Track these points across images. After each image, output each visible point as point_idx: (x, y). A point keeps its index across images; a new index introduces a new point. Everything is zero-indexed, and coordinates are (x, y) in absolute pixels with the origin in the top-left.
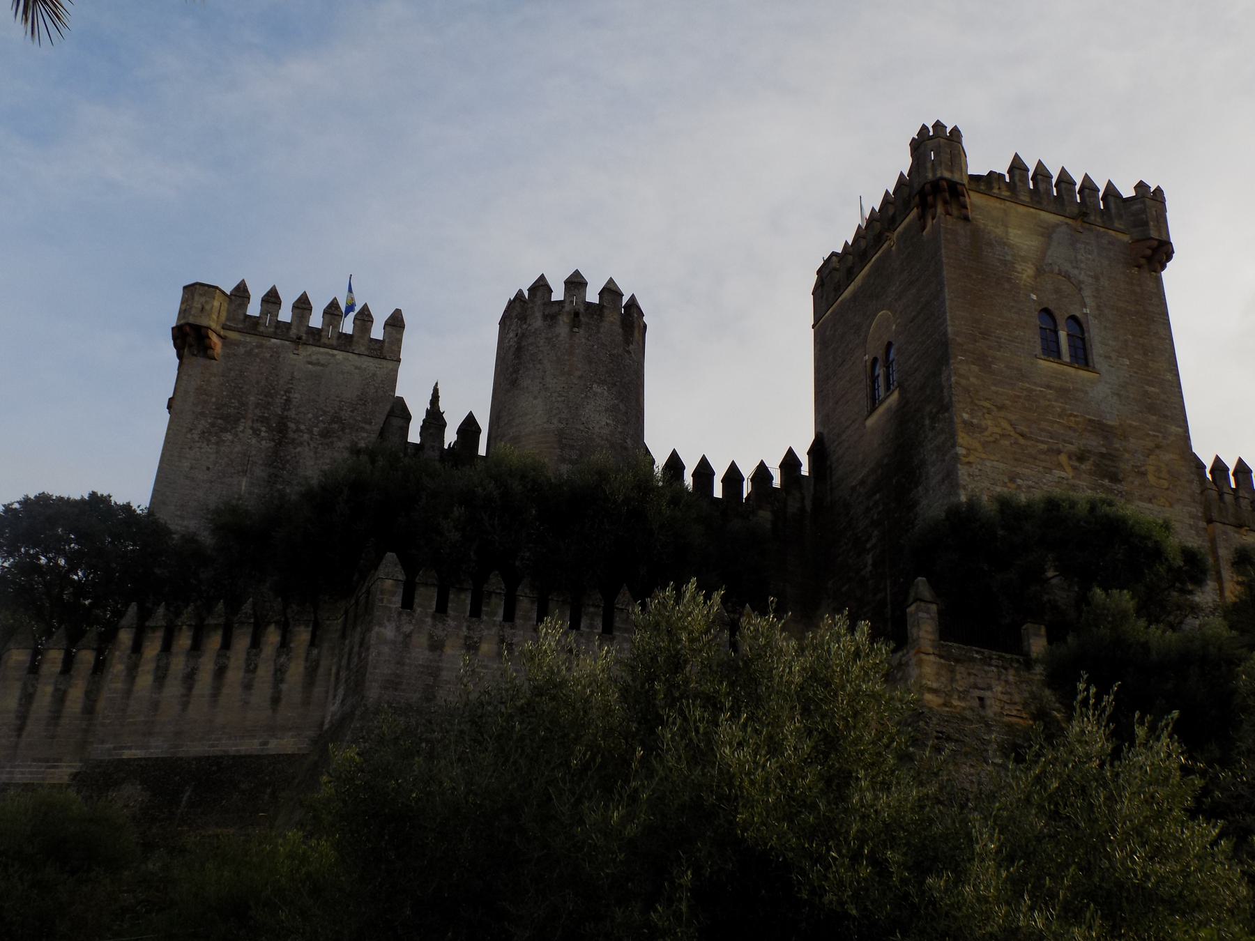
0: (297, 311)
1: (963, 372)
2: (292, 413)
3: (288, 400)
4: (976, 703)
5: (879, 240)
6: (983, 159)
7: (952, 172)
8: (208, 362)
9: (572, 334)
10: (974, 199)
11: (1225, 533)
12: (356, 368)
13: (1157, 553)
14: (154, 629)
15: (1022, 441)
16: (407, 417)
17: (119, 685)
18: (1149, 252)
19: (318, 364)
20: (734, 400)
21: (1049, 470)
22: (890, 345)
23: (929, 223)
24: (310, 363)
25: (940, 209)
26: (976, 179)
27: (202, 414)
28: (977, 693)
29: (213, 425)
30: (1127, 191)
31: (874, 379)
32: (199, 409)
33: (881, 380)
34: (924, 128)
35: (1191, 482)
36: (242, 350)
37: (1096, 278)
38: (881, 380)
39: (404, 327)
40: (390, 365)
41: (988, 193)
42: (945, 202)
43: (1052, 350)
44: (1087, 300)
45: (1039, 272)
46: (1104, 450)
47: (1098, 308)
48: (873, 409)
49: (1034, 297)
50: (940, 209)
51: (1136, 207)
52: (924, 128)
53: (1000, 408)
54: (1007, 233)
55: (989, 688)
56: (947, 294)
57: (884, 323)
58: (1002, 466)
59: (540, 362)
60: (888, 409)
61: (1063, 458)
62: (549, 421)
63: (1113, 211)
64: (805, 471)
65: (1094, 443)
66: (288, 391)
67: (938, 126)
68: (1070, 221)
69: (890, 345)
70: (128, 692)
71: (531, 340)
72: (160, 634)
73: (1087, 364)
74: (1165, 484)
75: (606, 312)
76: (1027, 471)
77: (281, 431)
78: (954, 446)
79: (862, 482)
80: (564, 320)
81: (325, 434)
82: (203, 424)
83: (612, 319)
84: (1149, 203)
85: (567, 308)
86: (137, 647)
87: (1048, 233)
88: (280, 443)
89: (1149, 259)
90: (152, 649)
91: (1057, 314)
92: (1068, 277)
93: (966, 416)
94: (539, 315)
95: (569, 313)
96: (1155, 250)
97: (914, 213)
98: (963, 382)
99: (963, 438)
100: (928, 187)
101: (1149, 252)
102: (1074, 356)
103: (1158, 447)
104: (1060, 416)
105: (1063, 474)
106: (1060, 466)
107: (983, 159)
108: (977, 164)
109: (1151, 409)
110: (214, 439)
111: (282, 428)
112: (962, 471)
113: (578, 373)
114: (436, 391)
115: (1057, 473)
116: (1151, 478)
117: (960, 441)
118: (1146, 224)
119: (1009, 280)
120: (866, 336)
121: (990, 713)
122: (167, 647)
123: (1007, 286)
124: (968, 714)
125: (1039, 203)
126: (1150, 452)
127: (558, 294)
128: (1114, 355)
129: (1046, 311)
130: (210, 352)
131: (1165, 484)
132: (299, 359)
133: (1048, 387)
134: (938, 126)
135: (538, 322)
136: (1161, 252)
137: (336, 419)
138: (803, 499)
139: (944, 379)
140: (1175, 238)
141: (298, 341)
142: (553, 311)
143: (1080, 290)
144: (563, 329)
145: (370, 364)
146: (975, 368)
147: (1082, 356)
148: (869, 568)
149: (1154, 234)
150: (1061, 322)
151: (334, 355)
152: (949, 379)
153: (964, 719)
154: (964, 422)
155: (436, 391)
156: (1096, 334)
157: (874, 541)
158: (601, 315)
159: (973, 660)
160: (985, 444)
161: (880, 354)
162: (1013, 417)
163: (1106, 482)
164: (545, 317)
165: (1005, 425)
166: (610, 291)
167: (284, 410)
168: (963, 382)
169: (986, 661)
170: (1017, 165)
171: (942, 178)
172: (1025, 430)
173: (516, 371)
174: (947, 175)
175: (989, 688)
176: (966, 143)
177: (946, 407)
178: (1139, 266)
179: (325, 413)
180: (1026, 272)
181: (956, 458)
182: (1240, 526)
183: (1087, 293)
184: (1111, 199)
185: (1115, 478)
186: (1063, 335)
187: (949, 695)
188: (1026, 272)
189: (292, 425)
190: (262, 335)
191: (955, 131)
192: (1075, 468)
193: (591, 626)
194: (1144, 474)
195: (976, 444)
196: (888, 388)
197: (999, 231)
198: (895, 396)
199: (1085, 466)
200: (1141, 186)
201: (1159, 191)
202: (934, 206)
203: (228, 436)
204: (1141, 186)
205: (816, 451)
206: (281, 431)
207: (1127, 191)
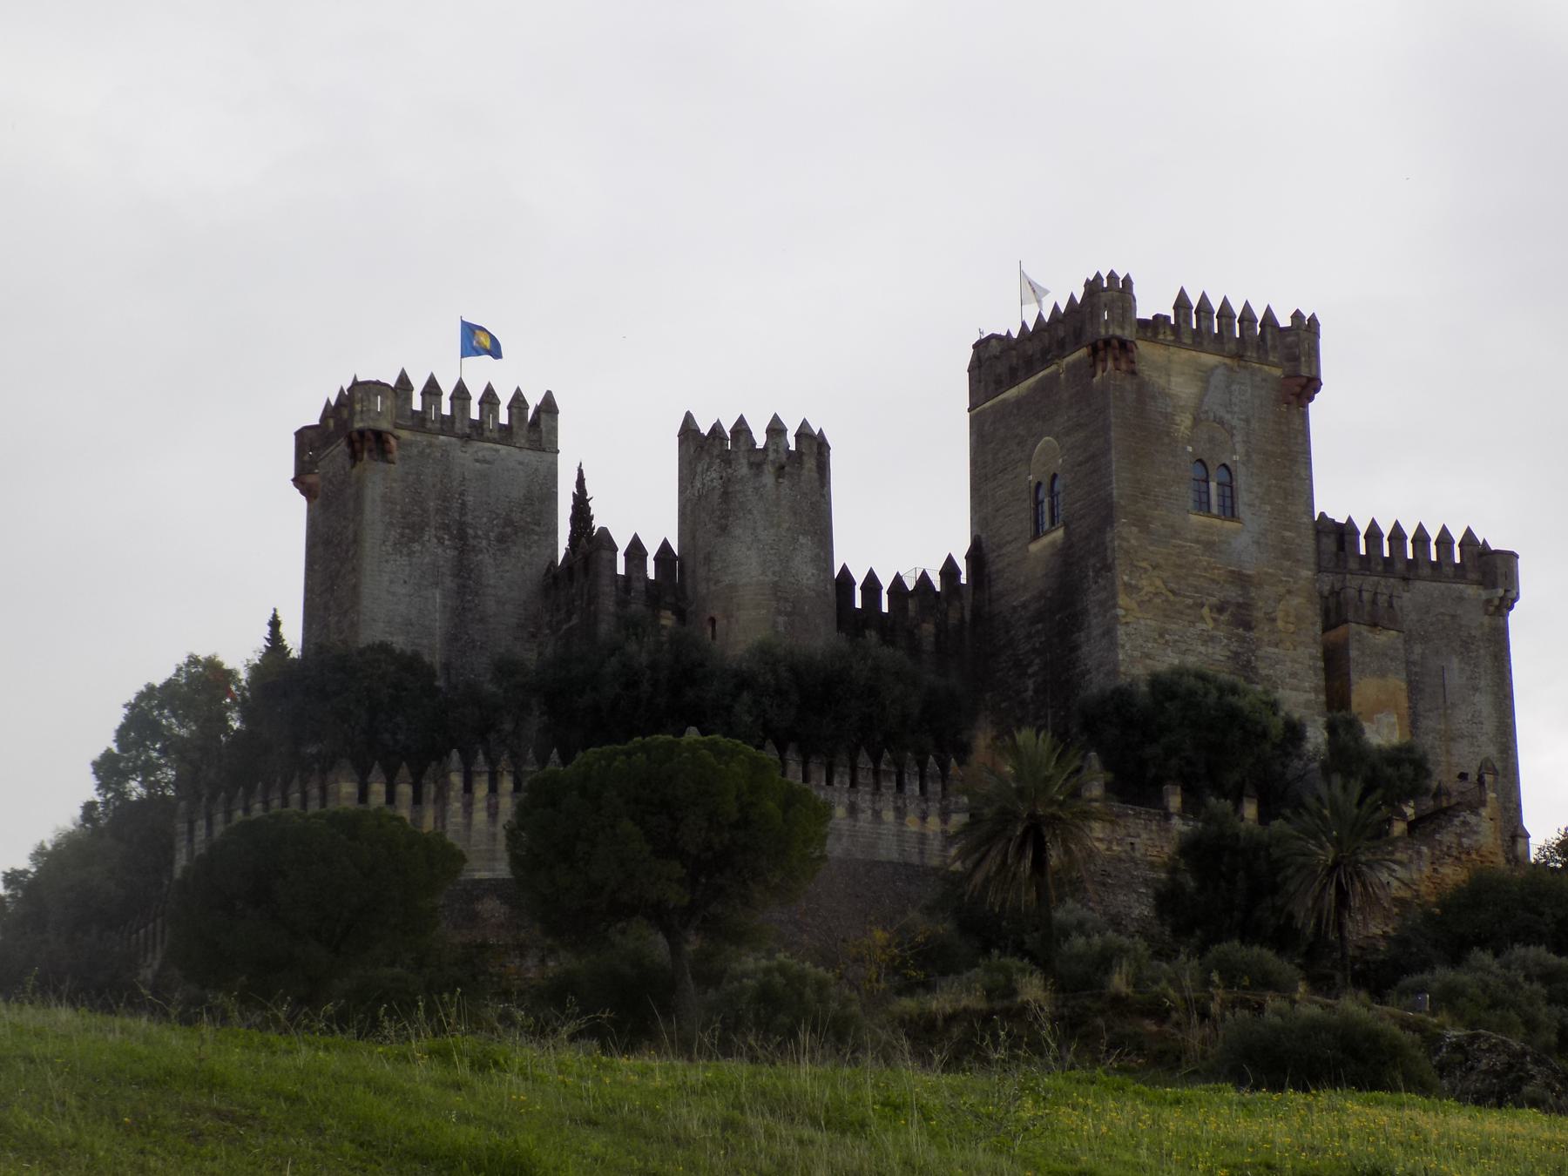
0: (457, 402)
1: (1125, 534)
2: (469, 518)
3: (464, 504)
4: (1128, 848)
5: (1046, 358)
6: (1152, 302)
7: (1123, 328)
8: (386, 466)
9: (778, 484)
10: (1143, 348)
11: (1359, 633)
12: (521, 463)
13: (1264, 735)
14: (480, 774)
15: (1172, 598)
16: (615, 549)
17: (459, 819)
18: (1298, 389)
19: (485, 461)
20: (903, 517)
21: (1192, 623)
22: (1055, 476)
23: (1099, 373)
24: (477, 461)
25: (1110, 364)
26: (1143, 323)
27: (391, 523)
28: (1130, 840)
29: (402, 535)
30: (1284, 321)
31: (1038, 503)
32: (387, 519)
33: (1046, 506)
34: (1098, 276)
35: (1313, 624)
36: (415, 451)
37: (1247, 421)
38: (1046, 506)
39: (556, 412)
40: (548, 457)
41: (1154, 339)
42: (1116, 359)
43: (1203, 506)
44: (1238, 446)
45: (1196, 421)
46: (1241, 600)
47: (1248, 454)
48: (1037, 536)
49: (1190, 449)
50: (1110, 364)
51: (1290, 339)
52: (1098, 276)
53: (1154, 568)
54: (1169, 382)
55: (1139, 836)
56: (1114, 455)
57: (1048, 453)
58: (1153, 623)
59: (750, 511)
60: (1053, 544)
61: (1206, 611)
62: (763, 573)
63: (1269, 343)
64: (963, 580)
65: (1233, 593)
66: (462, 494)
67: (1112, 276)
68: (1227, 361)
69: (1055, 476)
70: (468, 826)
71: (738, 487)
72: (485, 777)
73: (1233, 515)
74: (1292, 628)
75: (805, 458)
76: (1174, 627)
77: (461, 537)
78: (1115, 606)
79: (1024, 606)
80: (769, 469)
81: (501, 539)
82: (394, 534)
83: (810, 463)
84: (1306, 329)
85: (772, 456)
86: (468, 788)
87: (1205, 376)
88: (462, 552)
89: (1298, 396)
90: (481, 790)
91: (1209, 463)
92: (1222, 422)
93: (1126, 578)
94: (744, 461)
95: (773, 462)
96: (1304, 387)
97: (1082, 352)
98: (1125, 544)
99: (1122, 600)
100: (1100, 344)
101: (1298, 389)
102: (1222, 506)
103: (1289, 592)
104: (1205, 570)
105: (1204, 627)
106: (1202, 619)
107: (1152, 302)
108: (1144, 311)
110: (405, 551)
111: (462, 536)
112: (1121, 631)
113: (786, 525)
114: (580, 472)
115: (1200, 626)
116: (1280, 624)
117: (1121, 602)
118: (1296, 359)
119: (1168, 434)
120: (1030, 457)
121: (1138, 854)
122: (493, 789)
123: (1166, 440)
124: (1123, 855)
125: (1201, 344)
126: (1280, 599)
127: (760, 440)
128: (1257, 502)
129: (1200, 461)
130: (390, 457)
131: (1292, 628)
132: (466, 457)
133: (1197, 542)
134: (1112, 276)
135: (744, 470)
136: (1311, 385)
137: (509, 522)
138: (963, 608)
139: (1109, 536)
140: (1324, 376)
141: (466, 438)
142: (759, 460)
143: (1232, 435)
144: (768, 479)
145: (531, 457)
146: (1135, 530)
148: (1030, 693)
149: (1304, 371)
150: (1212, 472)
151: (497, 451)
152: (1112, 541)
153: (1120, 860)
154: (1125, 584)
155: (580, 472)
156: (1241, 481)
157: (1035, 668)
158: (801, 463)
159: (1127, 815)
160: (1141, 604)
161: (1046, 482)
162: (1165, 575)
163: (1241, 630)
164: (751, 465)
165: (1158, 583)
166: (804, 433)
167: (462, 515)
168: (1125, 544)
169: (1137, 816)
170: (1182, 303)
171: (1114, 337)
172: (1173, 586)
173: (726, 517)
174: (1118, 332)
175: (1139, 836)
176: (1136, 291)
177: (1108, 567)
178: (1288, 403)
179: (498, 515)
180: (1184, 422)
181: (1116, 617)
182: (1375, 625)
183: (1238, 438)
184: (1269, 329)
185: (1248, 626)
186: (1213, 485)
187: (1110, 842)
188: (1184, 422)
189: (470, 531)
190: (430, 432)
191: (1128, 281)
192: (1215, 620)
193: (842, 782)
194: (1274, 620)
195: (1134, 605)
196: (1053, 524)
197: (1162, 382)
198: (1059, 534)
199: (1224, 617)
200: (1297, 316)
201: (1313, 319)
202: (1104, 360)
203: (417, 547)
204: (1297, 316)
205: (976, 555)
206: (461, 537)
207: (1284, 321)
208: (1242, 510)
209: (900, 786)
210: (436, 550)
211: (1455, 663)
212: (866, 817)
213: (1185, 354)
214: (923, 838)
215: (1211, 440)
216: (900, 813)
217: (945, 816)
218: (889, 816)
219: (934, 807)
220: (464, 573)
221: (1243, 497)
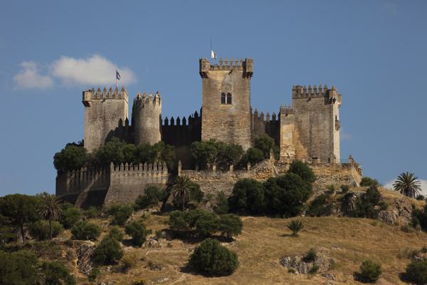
45: (222, 85)
65: (229, 119)
109: (242, 109)
137: (114, 114)
147: (229, 102)
208: (233, 102)
209: (153, 168)
210: (99, 122)
211: (321, 115)
212: (145, 176)
213: (220, 72)
214: (157, 178)
215: (226, 88)
216: (152, 174)
217: (162, 174)
218: (150, 175)
219: (160, 172)
220: (105, 126)
221: (233, 99)
